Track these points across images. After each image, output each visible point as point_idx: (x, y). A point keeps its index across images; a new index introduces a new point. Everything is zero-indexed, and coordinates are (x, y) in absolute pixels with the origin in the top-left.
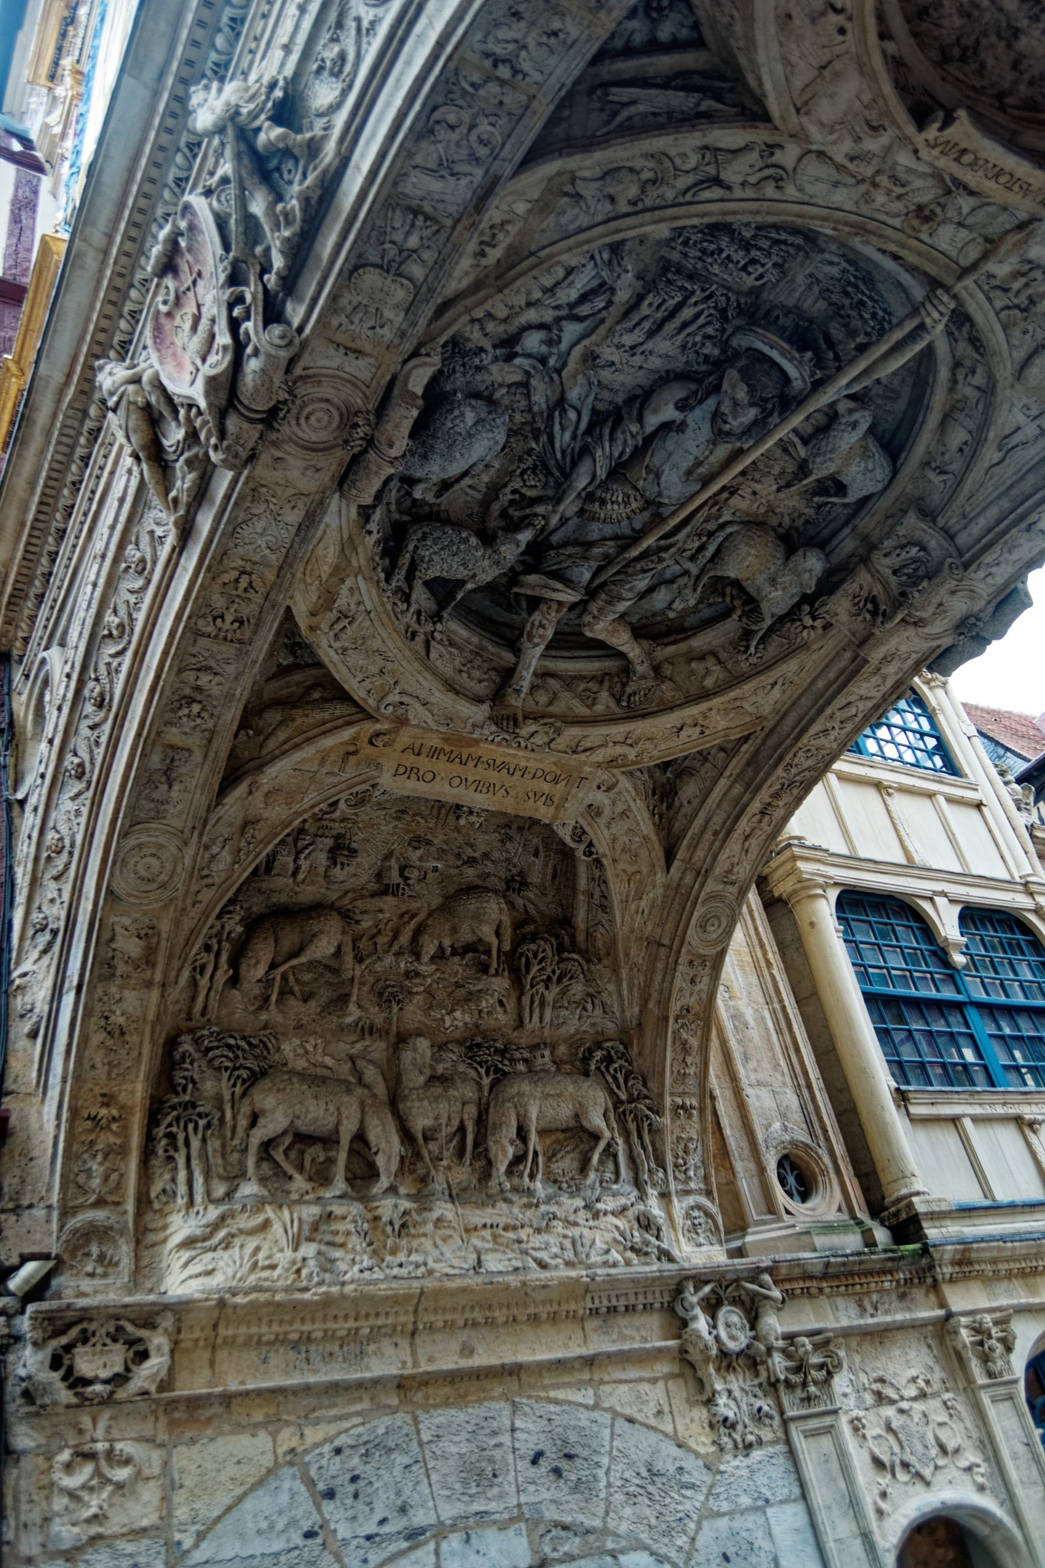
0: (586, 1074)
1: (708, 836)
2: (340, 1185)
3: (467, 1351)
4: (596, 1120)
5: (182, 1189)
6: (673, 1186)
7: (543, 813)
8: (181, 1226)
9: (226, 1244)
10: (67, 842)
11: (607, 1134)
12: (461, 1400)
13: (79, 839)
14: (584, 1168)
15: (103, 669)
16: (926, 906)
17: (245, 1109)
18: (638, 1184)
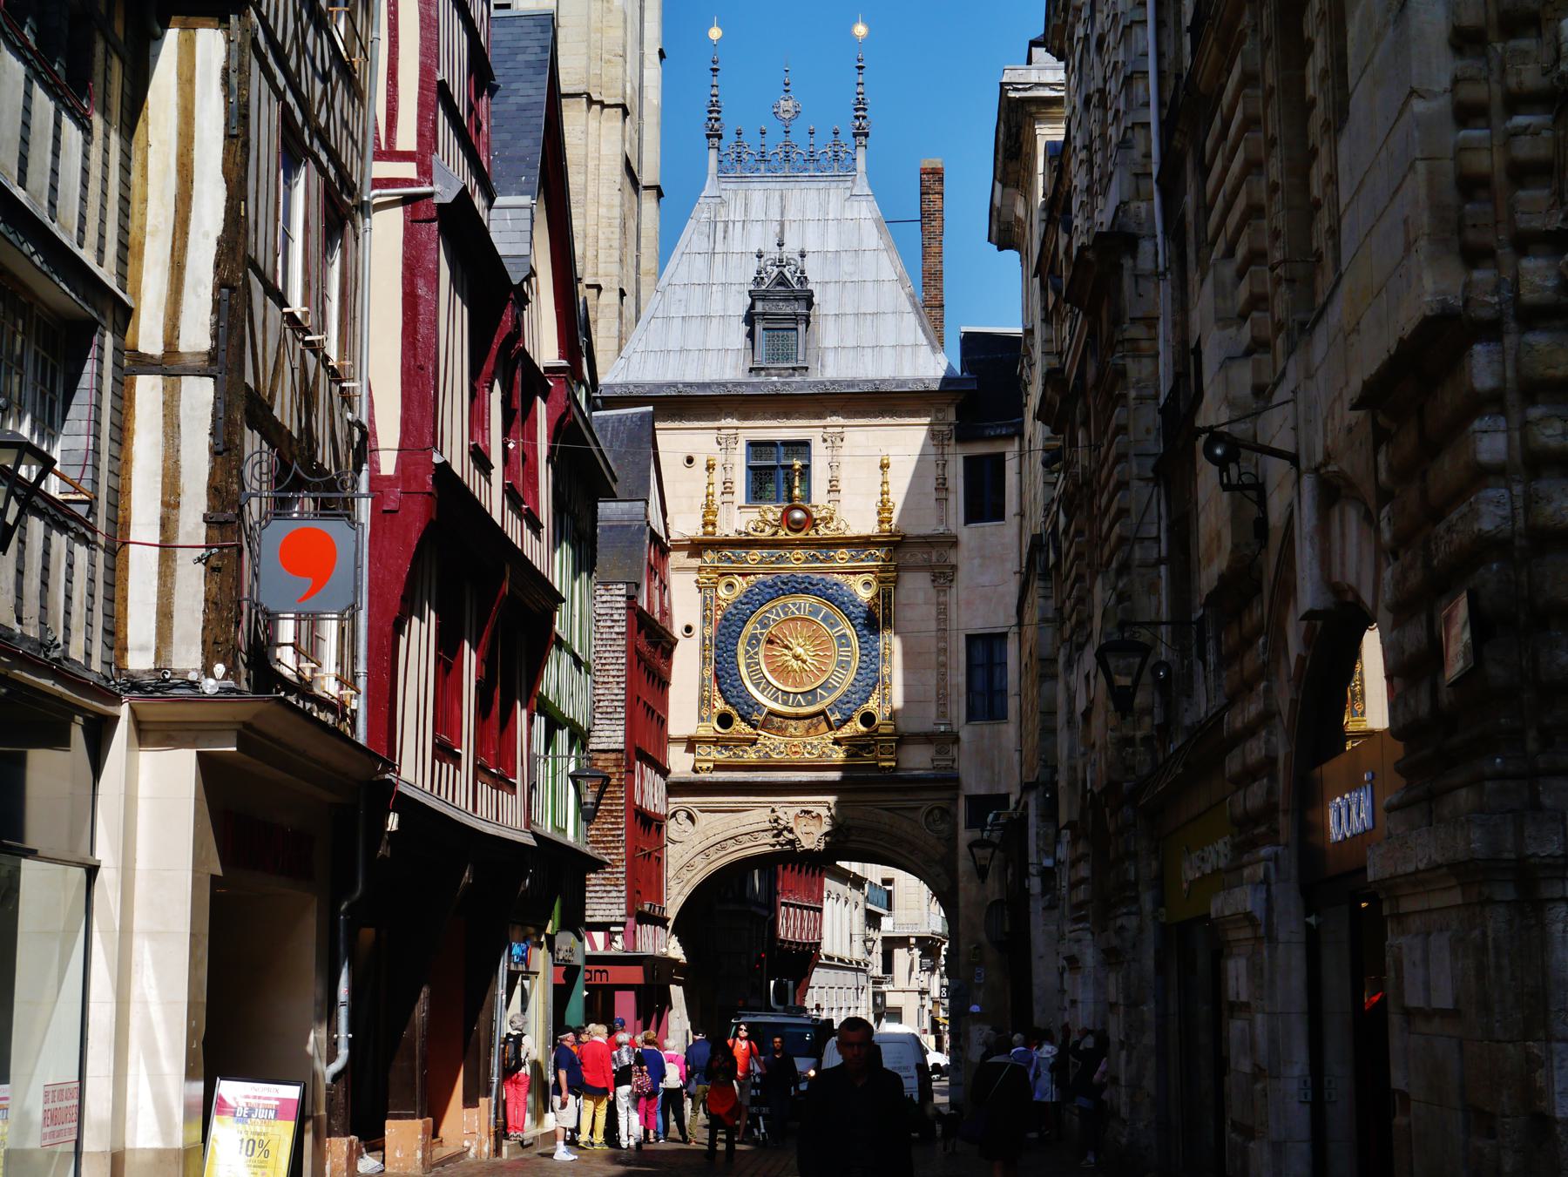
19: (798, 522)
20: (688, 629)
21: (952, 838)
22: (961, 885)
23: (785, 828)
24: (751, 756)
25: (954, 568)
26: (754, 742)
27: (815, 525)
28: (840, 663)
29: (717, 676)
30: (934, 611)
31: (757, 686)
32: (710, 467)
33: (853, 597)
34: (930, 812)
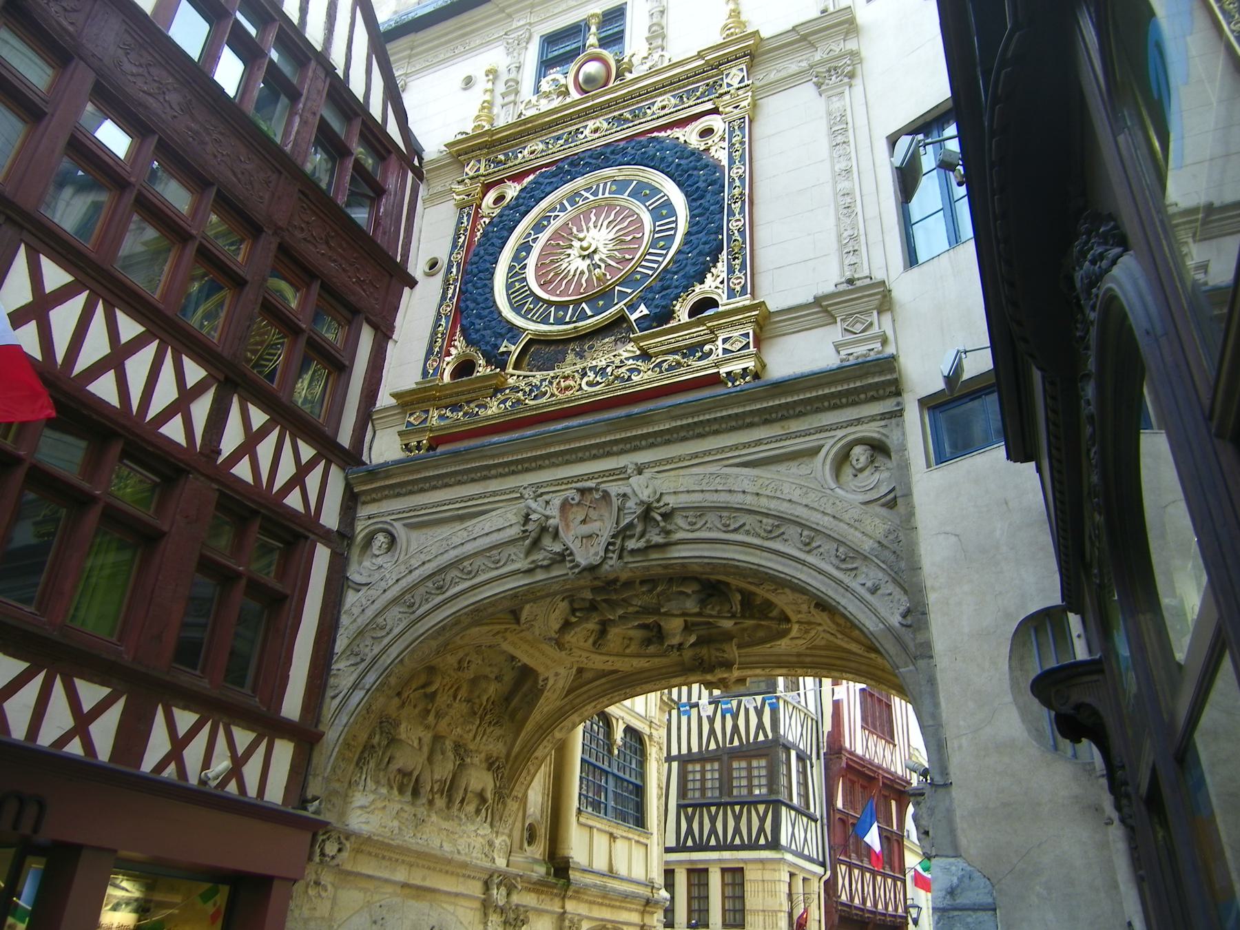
0: (489, 770)
1: (585, 696)
2: (408, 796)
3: (424, 879)
4: (489, 795)
5: (362, 783)
6: (501, 830)
7: (540, 669)
8: (359, 799)
9: (372, 812)
10: (388, 627)
11: (490, 801)
12: (417, 897)
13: (396, 631)
14: (478, 812)
15: (448, 578)
16: (614, 721)
17: (388, 754)
18: (492, 825)
19: (590, 80)
20: (433, 264)
21: (896, 500)
22: (932, 598)
23: (544, 530)
24: (494, 408)
25: (854, 55)
26: (498, 390)
27: (619, 75)
28: (653, 244)
29: (459, 311)
30: (823, 126)
31: (517, 309)
32: (492, 74)
33: (682, 150)
34: (843, 458)
